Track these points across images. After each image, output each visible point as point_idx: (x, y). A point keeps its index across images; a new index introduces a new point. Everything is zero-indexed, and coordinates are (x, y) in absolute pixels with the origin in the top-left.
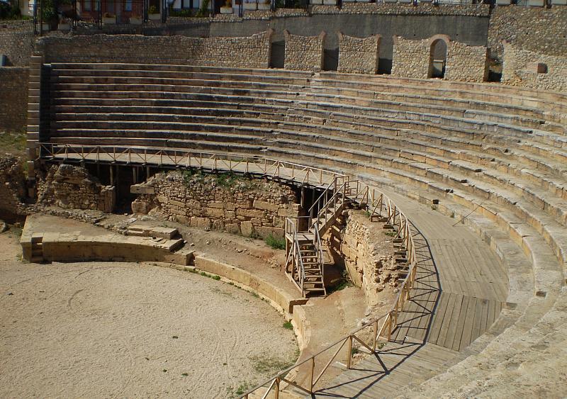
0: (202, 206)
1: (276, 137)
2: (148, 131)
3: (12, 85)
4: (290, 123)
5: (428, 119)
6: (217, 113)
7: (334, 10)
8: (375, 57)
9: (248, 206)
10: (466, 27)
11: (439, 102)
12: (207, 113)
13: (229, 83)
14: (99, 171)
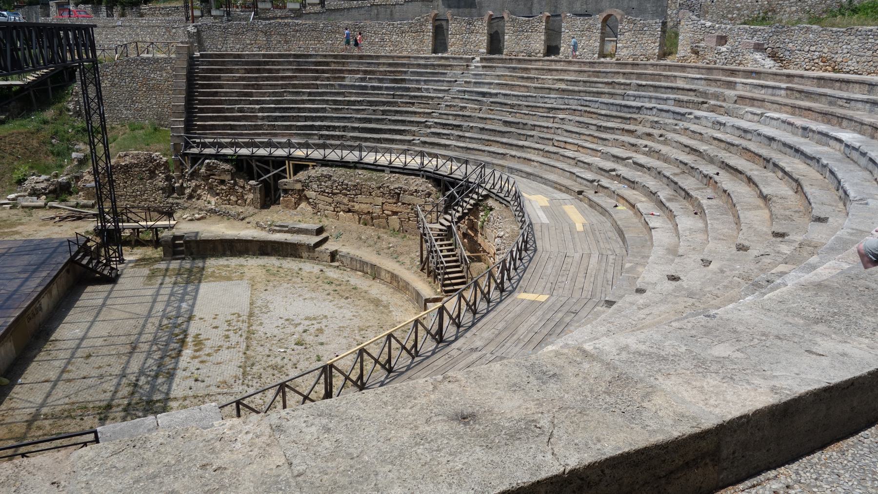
1: (430, 128)
2: (299, 124)
5: (587, 103)
6: (371, 103)
8: (543, 37)
9: (394, 201)
11: (600, 85)
12: (360, 103)
13: (385, 71)
14: (244, 167)
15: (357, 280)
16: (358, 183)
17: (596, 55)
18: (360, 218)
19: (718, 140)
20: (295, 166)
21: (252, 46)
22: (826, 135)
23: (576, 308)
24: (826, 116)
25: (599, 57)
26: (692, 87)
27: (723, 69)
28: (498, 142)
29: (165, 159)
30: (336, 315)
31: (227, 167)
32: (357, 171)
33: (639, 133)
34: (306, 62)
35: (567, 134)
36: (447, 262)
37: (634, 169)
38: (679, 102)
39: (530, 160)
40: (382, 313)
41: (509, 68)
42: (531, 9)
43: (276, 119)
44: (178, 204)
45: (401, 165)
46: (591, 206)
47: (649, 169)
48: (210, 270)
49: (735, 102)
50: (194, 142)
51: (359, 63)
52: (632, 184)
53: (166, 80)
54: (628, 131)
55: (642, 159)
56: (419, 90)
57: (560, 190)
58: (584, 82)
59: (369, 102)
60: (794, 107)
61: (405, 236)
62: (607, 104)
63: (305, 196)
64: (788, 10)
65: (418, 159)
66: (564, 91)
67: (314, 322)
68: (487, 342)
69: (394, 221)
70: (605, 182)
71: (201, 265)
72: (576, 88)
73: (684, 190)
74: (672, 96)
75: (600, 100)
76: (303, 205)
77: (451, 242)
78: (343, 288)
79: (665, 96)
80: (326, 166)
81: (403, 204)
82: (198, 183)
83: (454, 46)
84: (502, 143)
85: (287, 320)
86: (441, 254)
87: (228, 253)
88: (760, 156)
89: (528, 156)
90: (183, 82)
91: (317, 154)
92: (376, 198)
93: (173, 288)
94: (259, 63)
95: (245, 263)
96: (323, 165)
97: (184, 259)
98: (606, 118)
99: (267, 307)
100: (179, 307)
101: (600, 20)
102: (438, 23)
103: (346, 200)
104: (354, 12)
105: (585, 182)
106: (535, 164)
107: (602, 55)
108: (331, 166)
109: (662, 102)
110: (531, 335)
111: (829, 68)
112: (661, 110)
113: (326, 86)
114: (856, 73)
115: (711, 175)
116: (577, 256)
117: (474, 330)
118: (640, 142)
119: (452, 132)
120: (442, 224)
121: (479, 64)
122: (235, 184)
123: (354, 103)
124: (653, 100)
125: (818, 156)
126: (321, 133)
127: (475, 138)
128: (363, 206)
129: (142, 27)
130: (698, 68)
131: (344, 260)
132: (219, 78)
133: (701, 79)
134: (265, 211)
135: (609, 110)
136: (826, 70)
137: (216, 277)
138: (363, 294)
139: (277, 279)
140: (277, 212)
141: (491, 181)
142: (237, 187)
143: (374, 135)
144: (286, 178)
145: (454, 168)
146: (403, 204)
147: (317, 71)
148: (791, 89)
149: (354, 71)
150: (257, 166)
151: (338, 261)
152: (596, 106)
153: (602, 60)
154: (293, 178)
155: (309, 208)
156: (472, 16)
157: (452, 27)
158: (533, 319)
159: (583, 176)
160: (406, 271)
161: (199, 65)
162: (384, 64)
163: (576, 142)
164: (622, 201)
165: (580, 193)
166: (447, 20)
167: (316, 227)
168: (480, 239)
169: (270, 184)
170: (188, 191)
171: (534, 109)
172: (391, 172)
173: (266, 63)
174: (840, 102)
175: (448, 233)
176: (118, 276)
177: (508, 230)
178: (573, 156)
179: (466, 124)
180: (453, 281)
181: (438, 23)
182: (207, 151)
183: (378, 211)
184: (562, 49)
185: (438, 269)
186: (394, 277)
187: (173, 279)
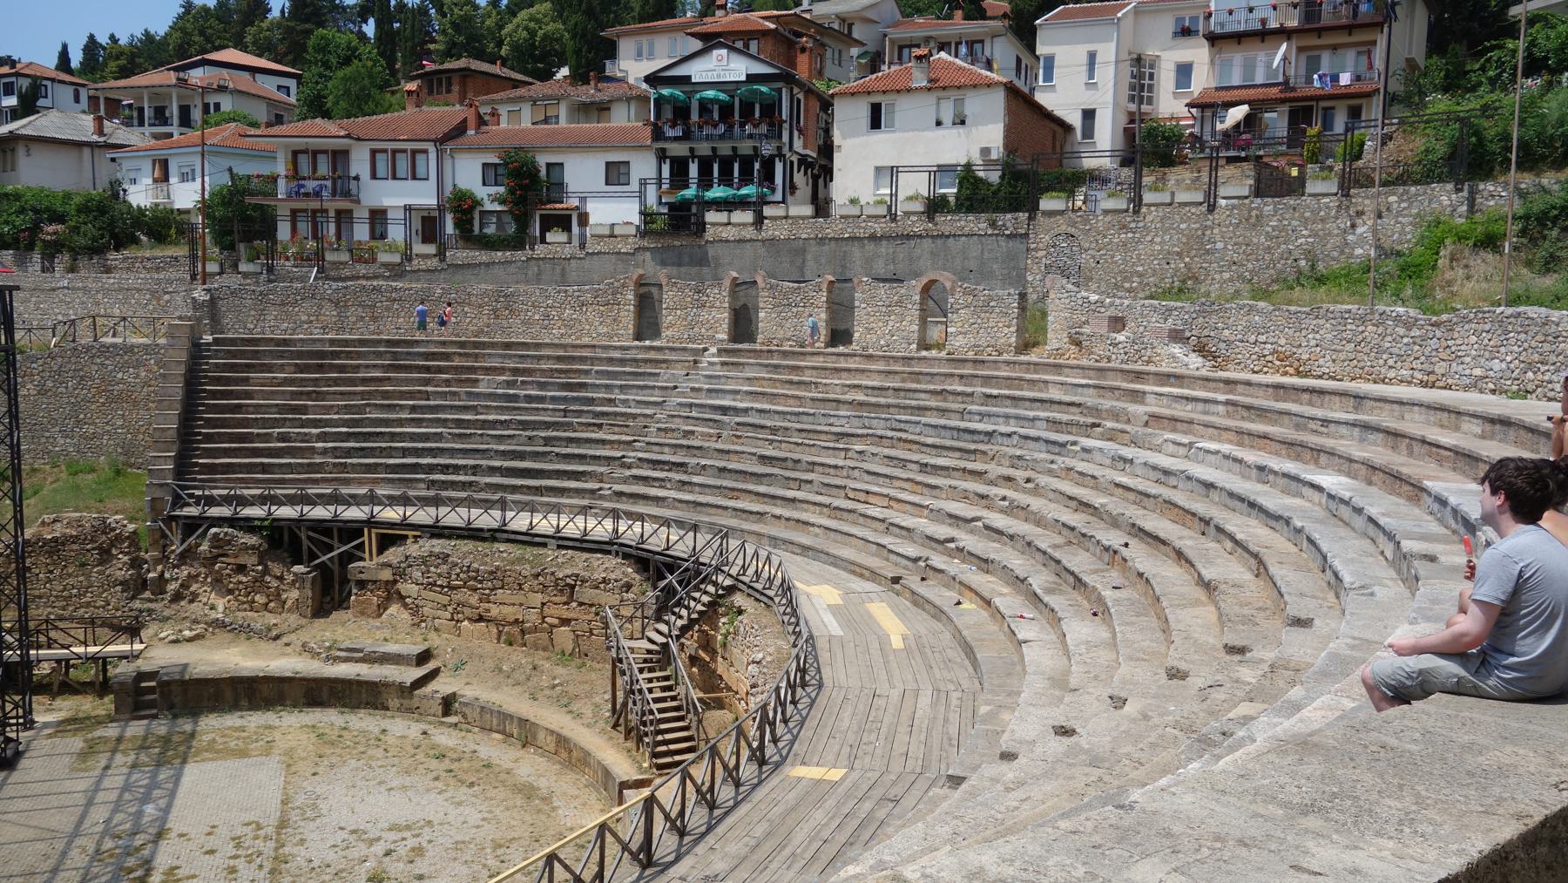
2: (392, 461)
3: (138, 376)
5: (902, 426)
6: (525, 425)
7: (750, 233)
9: (564, 599)
10: (986, 255)
11: (923, 396)
14: (284, 541)
15: (492, 749)
16: (498, 568)
18: (500, 632)
22: (1296, 479)
23: (897, 791)
24: (1292, 448)
25: (918, 349)
27: (1122, 371)
28: (750, 492)
29: (131, 527)
30: (450, 818)
31: (252, 540)
32: (496, 545)
33: (991, 476)
34: (408, 353)
35: (870, 478)
36: (661, 711)
38: (1054, 424)
39: (807, 523)
40: (539, 811)
41: (766, 366)
42: (802, 269)
43: (349, 453)
44: (150, 611)
45: (577, 534)
46: (915, 603)
47: (1011, 537)
49: (1146, 424)
50: (191, 496)
51: (504, 356)
52: (985, 564)
53: (146, 384)
54: (973, 473)
55: (999, 521)
56: (611, 402)
57: (861, 576)
59: (520, 422)
60: (1240, 432)
61: (584, 664)
62: (935, 427)
64: (1217, 276)
65: (608, 524)
66: (861, 404)
67: (407, 834)
68: (735, 862)
69: (564, 635)
70: (938, 561)
71: (188, 727)
72: (882, 401)
73: (1072, 573)
75: (923, 420)
76: (394, 609)
79: (1031, 414)
80: (439, 536)
82: (193, 572)
83: (673, 326)
84: (757, 494)
85: (354, 832)
86: (649, 696)
87: (245, 703)
88: (1194, 515)
89: (804, 516)
90: (176, 389)
91: (423, 516)
92: (531, 595)
93: (129, 774)
94: (321, 355)
95: (277, 723)
96: (433, 536)
97: (155, 717)
98: (934, 451)
99: (315, 807)
100: (140, 814)
102: (643, 290)
103: (474, 600)
105: (904, 562)
107: (924, 345)
108: (449, 537)
109: (1026, 423)
110: (816, 845)
111: (1291, 370)
112: (1026, 438)
113: (444, 395)
114: (1334, 378)
115: (1116, 547)
116: (895, 695)
119: (670, 475)
120: (651, 641)
121: (716, 360)
122: (266, 571)
124: (1012, 421)
125: (1286, 515)
126: (432, 477)
128: (507, 610)
129: (107, 291)
130: (1083, 368)
131: (467, 711)
132: (246, 381)
134: (320, 623)
135: (938, 436)
136: (1286, 373)
137: (217, 752)
138: (503, 776)
139: (338, 751)
140: (343, 624)
141: (740, 562)
142: (268, 579)
143: (532, 483)
144: (362, 559)
145: (673, 538)
147: (428, 369)
148: (1234, 404)
149: (496, 368)
150: (309, 538)
151: (456, 713)
152: (918, 430)
153: (924, 353)
155: (405, 615)
157: (669, 297)
158: (819, 815)
159: (900, 550)
160: (585, 731)
162: (549, 358)
163: (885, 491)
164: (967, 592)
165: (896, 580)
167: (417, 649)
168: (721, 667)
169: (332, 572)
170: (172, 587)
171: (811, 435)
172: (559, 547)
173: (335, 355)
174: (1312, 425)
175: (662, 657)
176: (18, 755)
178: (881, 516)
180: (672, 747)
181: (643, 290)
182: (215, 512)
184: (856, 335)
185: (644, 724)
186: (562, 742)
187: (132, 757)
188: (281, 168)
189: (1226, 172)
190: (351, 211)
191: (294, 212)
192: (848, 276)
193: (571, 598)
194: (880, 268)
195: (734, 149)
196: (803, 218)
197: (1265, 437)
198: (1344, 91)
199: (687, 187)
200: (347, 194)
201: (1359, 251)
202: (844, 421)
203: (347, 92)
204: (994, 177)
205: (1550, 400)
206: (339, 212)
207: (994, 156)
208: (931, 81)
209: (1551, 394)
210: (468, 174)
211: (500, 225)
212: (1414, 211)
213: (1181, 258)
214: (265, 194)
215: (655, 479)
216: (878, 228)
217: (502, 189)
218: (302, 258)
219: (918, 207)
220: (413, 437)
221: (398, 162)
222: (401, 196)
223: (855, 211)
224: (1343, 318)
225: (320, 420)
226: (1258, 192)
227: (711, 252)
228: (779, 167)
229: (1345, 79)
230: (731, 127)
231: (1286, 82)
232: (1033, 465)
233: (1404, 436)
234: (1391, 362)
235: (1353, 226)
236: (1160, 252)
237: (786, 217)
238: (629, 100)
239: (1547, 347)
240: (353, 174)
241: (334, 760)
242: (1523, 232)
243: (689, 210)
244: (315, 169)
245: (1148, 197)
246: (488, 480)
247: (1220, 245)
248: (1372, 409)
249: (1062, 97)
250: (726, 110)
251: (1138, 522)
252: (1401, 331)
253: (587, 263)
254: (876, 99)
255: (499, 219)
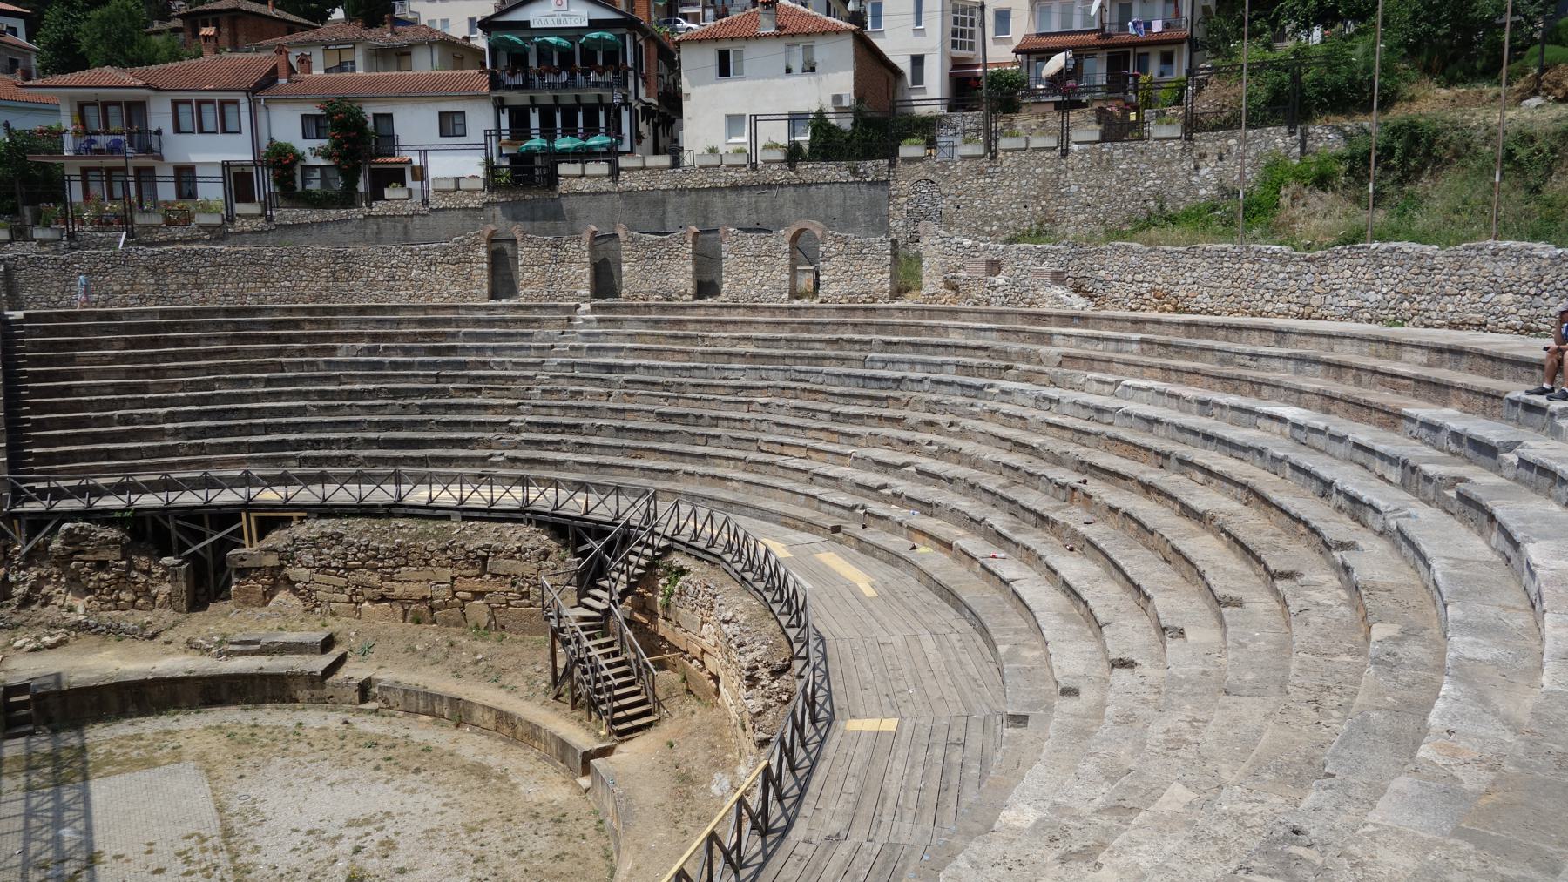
0: (383, 580)
1: (518, 431)
2: (254, 439)
4: (544, 402)
5: (803, 376)
6: (395, 393)
7: (606, 184)
8: (690, 268)
9: (477, 571)
10: (849, 203)
11: (817, 345)
12: (373, 394)
13: (415, 334)
14: (149, 533)
15: (423, 731)
16: (400, 545)
17: (786, 295)
18: (405, 612)
19: (1057, 426)
20: (259, 519)
21: (132, 296)
22: (1250, 411)
26: (980, 343)
27: (1022, 314)
30: (409, 807)
31: (112, 533)
32: (394, 521)
34: (254, 322)
35: (780, 430)
36: (616, 676)
37: (919, 481)
39: (724, 479)
40: (499, 790)
41: (646, 321)
42: (662, 221)
43: (204, 432)
45: (482, 504)
46: (862, 551)
47: (951, 481)
48: (101, 750)
49: (1060, 365)
50: (32, 489)
51: (360, 322)
52: (928, 508)
56: (485, 365)
57: (795, 527)
58: (787, 340)
59: (391, 391)
60: (1165, 369)
61: (503, 637)
63: (287, 578)
65: (517, 492)
66: (754, 356)
67: (369, 829)
70: (876, 507)
71: (75, 741)
72: (777, 352)
73: (1034, 512)
74: (952, 359)
75: (825, 369)
76: (282, 596)
77: (610, 639)
78: (403, 751)
79: (939, 359)
81: (495, 576)
82: (43, 572)
83: (530, 285)
84: (663, 452)
85: (310, 832)
88: (1149, 449)
89: (719, 471)
91: (307, 495)
93: (27, 798)
95: (175, 727)
96: (321, 516)
97: (31, 734)
98: (842, 400)
99: (256, 812)
100: (58, 840)
101: (788, 239)
102: (496, 246)
103: (375, 579)
104: (331, 230)
105: (838, 511)
106: (735, 484)
108: (339, 516)
109: (933, 369)
111: (1169, 307)
112: (939, 383)
113: (300, 366)
115: (1075, 484)
116: (897, 640)
117: (809, 800)
118: (918, 436)
119: (565, 437)
122: (131, 566)
123: (361, 394)
124: (918, 367)
125: (1259, 445)
127: (609, 447)
128: (412, 587)
130: (980, 312)
133: (991, 330)
136: (1164, 310)
137: (120, 764)
138: (448, 759)
139: (256, 750)
140: (226, 616)
143: (408, 452)
146: (495, 576)
147: (277, 339)
148: (1150, 342)
149: (353, 335)
150: (178, 527)
151: (374, 698)
152: (820, 379)
153: (796, 303)
154: (257, 546)
155: (296, 601)
156: (558, 235)
157: (525, 253)
158: (898, 765)
159: (834, 500)
161: (23, 335)
162: (409, 321)
163: (802, 442)
164: (918, 537)
165: (836, 529)
166: (514, 242)
167: (319, 636)
168: (663, 628)
169: (205, 561)
171: (707, 390)
172: (464, 518)
174: (1239, 360)
175: (600, 624)
177: (740, 607)
178: (803, 467)
179: (587, 422)
180: (630, 712)
181: (496, 246)
182: (64, 505)
183: (443, 593)
184: (725, 286)
186: (503, 718)
187: (22, 780)
188: (66, 121)
189: (1074, 116)
190: (152, 169)
191: (85, 171)
192: (712, 226)
193: (484, 570)
194: (743, 217)
195: (577, 97)
196: (661, 168)
197: (1196, 372)
198: (1155, 38)
199: (529, 138)
200: (147, 150)
201: (1203, 192)
202: (739, 374)
203: (105, 35)
204: (847, 124)
205: (1427, 326)
206: (138, 170)
207: (846, 103)
208: (778, 28)
209: (1428, 322)
210: (286, 126)
211: (324, 180)
212: (1252, 153)
213: (1038, 202)
214: (50, 152)
215: (549, 443)
216: (739, 177)
217: (325, 142)
218: (101, 221)
219: (779, 155)
220: (273, 412)
221: (200, 114)
222: (211, 153)
223: (714, 161)
224: (1220, 256)
225: (165, 399)
226: (1104, 139)
227: (566, 205)
228: (625, 116)
229: (1157, 26)
230: (572, 75)
231: (1103, 28)
232: (952, 409)
233: (1350, 367)
234: (1267, 296)
235: (1197, 168)
236: (1017, 196)
237: (644, 168)
238: (431, 44)
239: (1422, 278)
240: (153, 126)
241: (257, 760)
242: (1350, 171)
243: (532, 161)
244: (106, 125)
245: (1004, 143)
246: (367, 453)
247: (1074, 189)
248: (1296, 343)
249: (895, 43)
250: (566, 57)
251: (1088, 459)
252: (1277, 267)
253: (431, 220)
254: (724, 46)
255: (323, 174)
